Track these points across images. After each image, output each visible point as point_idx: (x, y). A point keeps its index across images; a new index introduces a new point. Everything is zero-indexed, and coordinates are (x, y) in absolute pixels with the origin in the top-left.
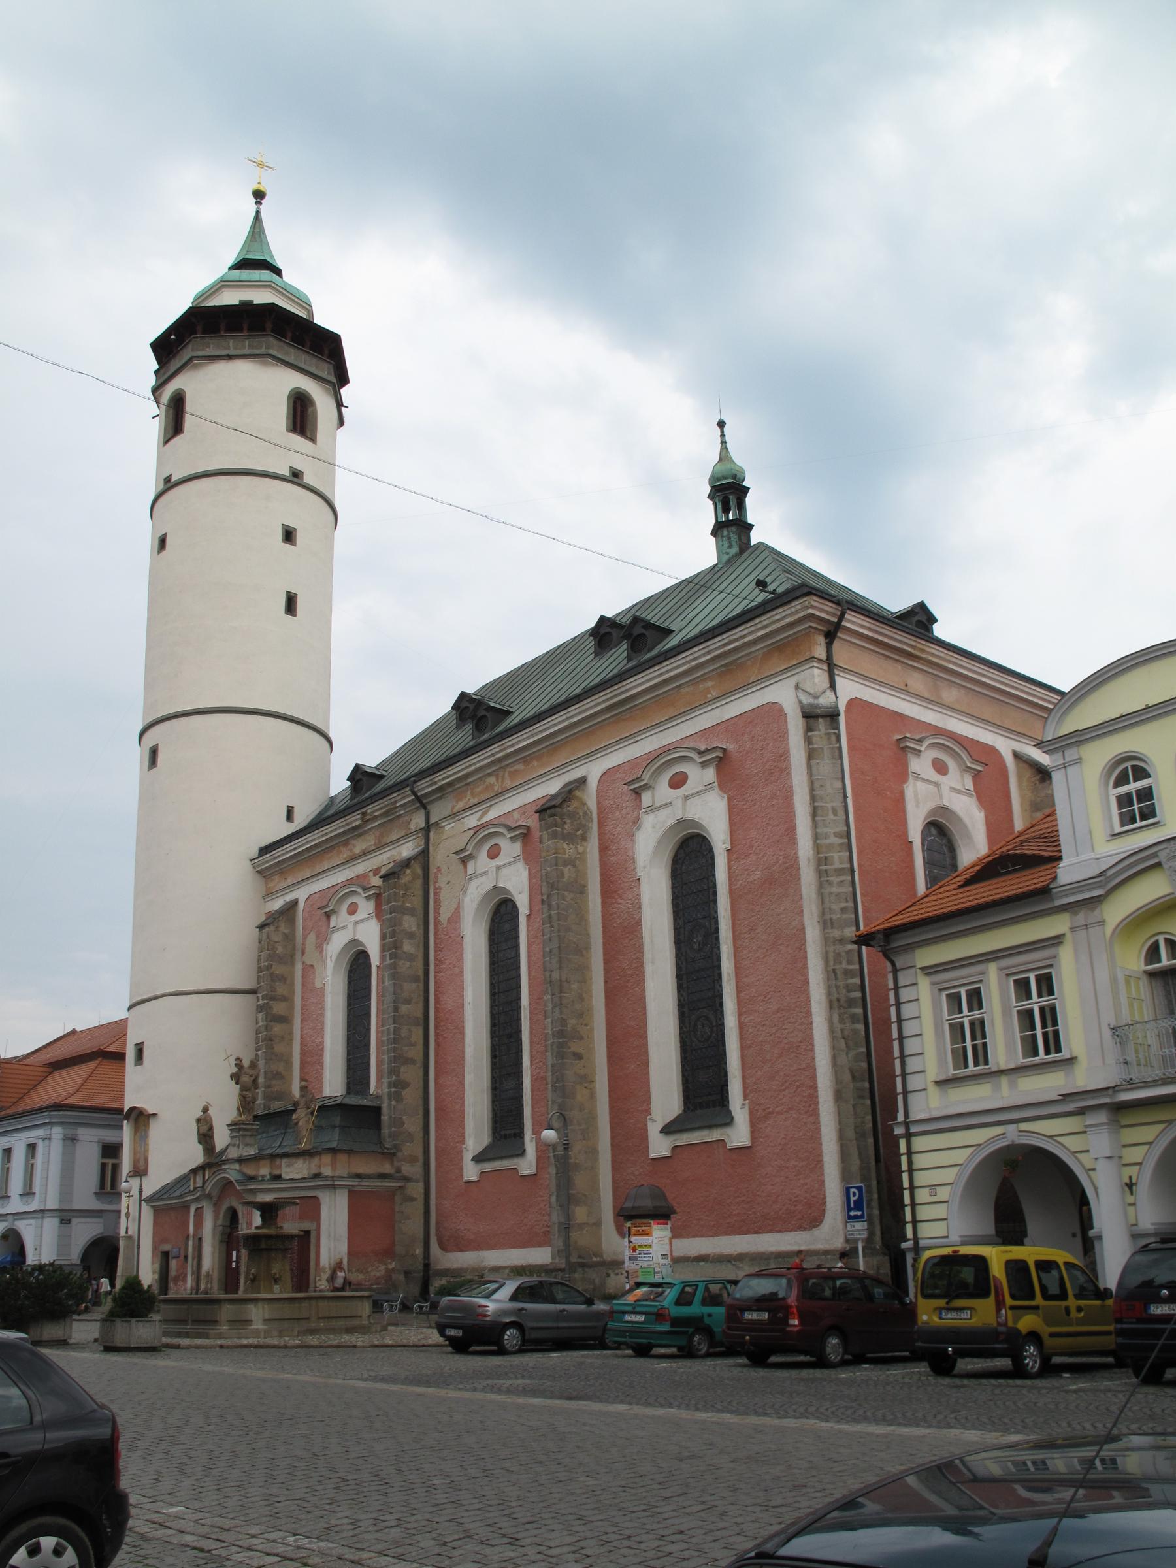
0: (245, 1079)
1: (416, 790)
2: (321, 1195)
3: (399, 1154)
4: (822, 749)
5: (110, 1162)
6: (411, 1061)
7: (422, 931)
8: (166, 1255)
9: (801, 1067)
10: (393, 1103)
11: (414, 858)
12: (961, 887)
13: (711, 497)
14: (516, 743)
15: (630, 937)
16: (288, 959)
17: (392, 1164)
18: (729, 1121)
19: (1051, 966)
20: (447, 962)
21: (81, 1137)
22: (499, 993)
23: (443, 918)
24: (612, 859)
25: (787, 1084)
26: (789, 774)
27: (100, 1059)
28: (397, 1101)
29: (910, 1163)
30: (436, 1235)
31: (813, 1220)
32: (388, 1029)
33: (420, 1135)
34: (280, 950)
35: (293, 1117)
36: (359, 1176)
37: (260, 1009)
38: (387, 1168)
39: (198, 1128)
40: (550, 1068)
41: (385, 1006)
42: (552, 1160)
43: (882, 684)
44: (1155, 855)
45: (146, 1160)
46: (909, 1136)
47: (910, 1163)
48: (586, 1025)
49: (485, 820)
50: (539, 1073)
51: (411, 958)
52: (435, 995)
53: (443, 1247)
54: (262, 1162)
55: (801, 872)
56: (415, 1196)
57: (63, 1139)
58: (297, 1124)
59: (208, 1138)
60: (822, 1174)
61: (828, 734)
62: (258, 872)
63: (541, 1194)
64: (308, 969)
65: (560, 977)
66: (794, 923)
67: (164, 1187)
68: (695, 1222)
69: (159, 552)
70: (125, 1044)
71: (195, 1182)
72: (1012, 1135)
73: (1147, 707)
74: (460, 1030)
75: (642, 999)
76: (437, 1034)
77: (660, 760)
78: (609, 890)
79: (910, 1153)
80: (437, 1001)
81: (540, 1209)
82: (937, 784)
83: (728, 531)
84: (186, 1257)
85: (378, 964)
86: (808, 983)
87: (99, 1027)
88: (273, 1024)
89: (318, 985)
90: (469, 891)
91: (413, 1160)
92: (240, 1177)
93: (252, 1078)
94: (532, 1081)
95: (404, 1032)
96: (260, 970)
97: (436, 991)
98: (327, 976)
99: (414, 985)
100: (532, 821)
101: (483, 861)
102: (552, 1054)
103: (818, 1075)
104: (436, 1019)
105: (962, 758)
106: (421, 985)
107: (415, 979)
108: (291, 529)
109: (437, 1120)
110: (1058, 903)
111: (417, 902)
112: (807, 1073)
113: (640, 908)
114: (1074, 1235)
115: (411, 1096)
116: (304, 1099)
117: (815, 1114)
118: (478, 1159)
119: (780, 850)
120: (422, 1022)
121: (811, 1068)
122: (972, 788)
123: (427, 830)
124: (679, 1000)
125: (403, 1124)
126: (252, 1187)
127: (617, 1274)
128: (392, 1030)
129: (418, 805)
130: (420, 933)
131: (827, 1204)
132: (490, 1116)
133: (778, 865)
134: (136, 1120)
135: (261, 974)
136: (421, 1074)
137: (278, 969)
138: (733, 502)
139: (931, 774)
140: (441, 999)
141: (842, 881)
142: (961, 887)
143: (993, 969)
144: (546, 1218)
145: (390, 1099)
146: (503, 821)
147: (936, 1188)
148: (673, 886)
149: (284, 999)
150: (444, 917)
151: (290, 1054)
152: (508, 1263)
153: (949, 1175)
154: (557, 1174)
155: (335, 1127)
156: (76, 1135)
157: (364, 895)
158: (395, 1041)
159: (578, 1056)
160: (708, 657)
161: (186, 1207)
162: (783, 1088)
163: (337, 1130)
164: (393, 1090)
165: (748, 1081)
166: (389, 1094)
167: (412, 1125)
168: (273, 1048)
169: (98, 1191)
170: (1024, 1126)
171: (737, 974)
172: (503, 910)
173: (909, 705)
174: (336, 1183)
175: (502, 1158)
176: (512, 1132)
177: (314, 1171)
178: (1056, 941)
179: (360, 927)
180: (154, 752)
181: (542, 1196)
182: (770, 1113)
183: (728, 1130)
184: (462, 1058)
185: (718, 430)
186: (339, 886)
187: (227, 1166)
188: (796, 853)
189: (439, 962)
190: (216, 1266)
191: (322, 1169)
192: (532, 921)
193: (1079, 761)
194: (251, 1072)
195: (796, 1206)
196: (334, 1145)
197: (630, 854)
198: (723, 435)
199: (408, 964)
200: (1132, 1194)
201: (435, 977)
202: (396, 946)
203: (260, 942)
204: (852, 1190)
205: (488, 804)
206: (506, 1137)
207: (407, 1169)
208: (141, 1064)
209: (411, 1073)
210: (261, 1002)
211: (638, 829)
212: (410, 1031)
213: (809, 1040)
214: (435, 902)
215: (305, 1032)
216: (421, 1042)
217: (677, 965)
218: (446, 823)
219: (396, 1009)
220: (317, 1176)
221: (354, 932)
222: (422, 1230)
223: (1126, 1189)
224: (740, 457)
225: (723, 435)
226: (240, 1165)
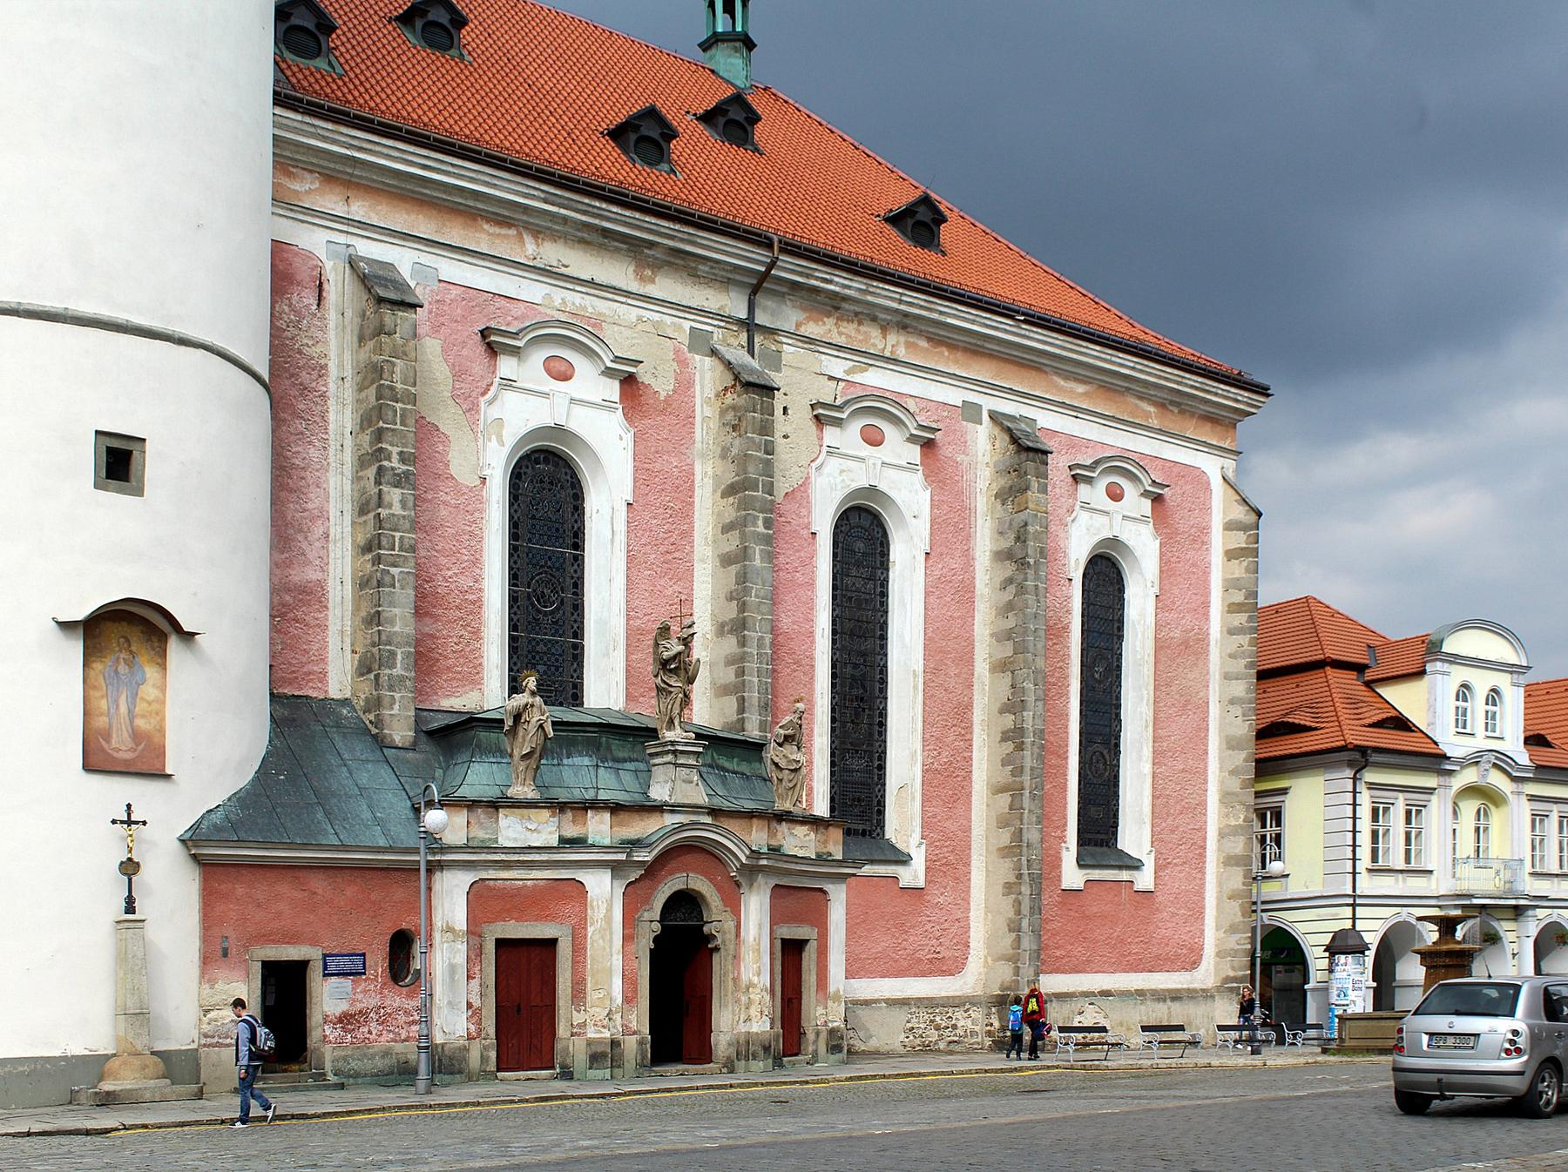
2: (828, 887)
42: (1026, 878)
102: (1032, 754)
117: (1202, 871)
121: (1202, 830)
152: (887, 995)
172: (854, 520)
182: (1169, 863)
183: (1135, 873)
213: (1203, 804)
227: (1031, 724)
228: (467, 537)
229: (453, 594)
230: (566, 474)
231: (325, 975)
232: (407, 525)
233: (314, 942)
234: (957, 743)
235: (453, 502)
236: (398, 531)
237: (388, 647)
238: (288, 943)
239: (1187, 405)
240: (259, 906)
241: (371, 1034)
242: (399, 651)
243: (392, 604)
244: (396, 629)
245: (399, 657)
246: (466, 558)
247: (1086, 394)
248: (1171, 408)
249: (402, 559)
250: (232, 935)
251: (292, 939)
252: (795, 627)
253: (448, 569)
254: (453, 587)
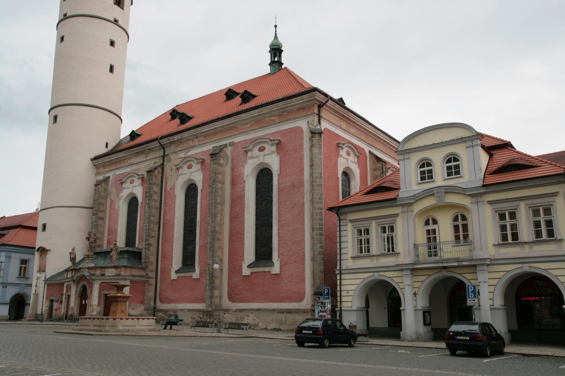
0: (92, 239)
1: (160, 142)
3: (148, 269)
4: (316, 144)
5: (23, 266)
6: (153, 237)
7: (160, 192)
8: (52, 301)
9: (300, 249)
10: (147, 251)
11: (159, 166)
12: (363, 195)
13: (270, 52)
14: (202, 130)
15: (240, 201)
16: (106, 198)
17: (145, 272)
18: (272, 265)
19: (394, 223)
21: (13, 257)
22: (188, 215)
23: (168, 188)
24: (235, 173)
25: (294, 254)
26: (303, 151)
27: (20, 228)
28: (148, 250)
29: (340, 283)
30: (159, 297)
31: (300, 298)
32: (146, 225)
33: (155, 263)
34: (102, 194)
35: (111, 254)
36: (134, 276)
37: (94, 214)
38: (143, 273)
39: (70, 256)
40: (209, 243)
41: (145, 217)
42: (208, 274)
43: (334, 124)
44: (433, 191)
45: (45, 266)
46: (341, 274)
47: (340, 283)
48: (222, 229)
49: (187, 155)
50: (202, 244)
51: (155, 201)
52: (164, 214)
53: (161, 301)
54: (98, 269)
55: (305, 184)
56: (152, 284)
57: (6, 257)
58: (112, 256)
59: (74, 260)
60: (305, 284)
61: (319, 139)
62: (94, 165)
63: (201, 285)
64: (112, 202)
65: (215, 212)
66: (301, 201)
67: (52, 276)
68: (257, 297)
69: (60, 42)
70: (37, 224)
71: (67, 275)
72: (377, 276)
73: (434, 144)
74: (172, 227)
75: (243, 222)
76: (163, 228)
77: (255, 141)
78: (234, 183)
79: (340, 280)
80: (164, 217)
82: (347, 159)
83: (275, 64)
84: (61, 302)
85: (141, 202)
86: (304, 221)
87: (16, 216)
88: (99, 220)
89: (116, 208)
90: (179, 179)
91: (152, 271)
92: (88, 274)
93: (94, 239)
94: (199, 247)
95: (152, 226)
96: (94, 200)
97: (164, 213)
98: (120, 205)
99: (156, 211)
100: (208, 159)
101: (185, 170)
102: (210, 238)
103: (305, 252)
104: (163, 223)
105: (355, 152)
106: (159, 211)
107: (157, 209)
108: (113, 41)
109: (162, 258)
110: (398, 203)
111: (159, 182)
112: (301, 251)
113: (244, 191)
114: (385, 308)
115: (153, 249)
116: (115, 248)
118: (177, 272)
119: (298, 176)
120: (158, 223)
122: (357, 162)
123: (164, 156)
124: (256, 223)
125: (150, 258)
126: (94, 278)
127: (228, 314)
128: (147, 225)
129: (161, 147)
130: (159, 192)
131: (306, 294)
132: (182, 257)
133: (296, 181)
134: (41, 252)
135: (95, 202)
136: (156, 241)
137: (102, 201)
138: (278, 55)
139: (346, 156)
140: (166, 216)
141: (320, 189)
142: (363, 195)
143: (374, 223)
144: (202, 293)
145: (145, 250)
146: (194, 156)
147: (349, 291)
148: (257, 185)
149: (103, 211)
150: (168, 188)
151: (104, 231)
152: (187, 308)
153: (354, 287)
154: (209, 279)
155: (125, 258)
156: (11, 256)
157: (137, 177)
158: (149, 229)
159: (219, 240)
160: (277, 108)
161: (63, 284)
162: (293, 255)
163: (126, 259)
164: (147, 246)
165: (280, 252)
166: (145, 248)
167: (153, 259)
168: (98, 229)
169: (18, 276)
170: (380, 273)
171: (279, 216)
172: (191, 187)
173: (341, 132)
174: (126, 278)
175: (186, 272)
176: (190, 263)
177: (118, 273)
178: (397, 215)
179: (134, 188)
180: (56, 118)
182: (288, 263)
183: (272, 268)
184: (173, 237)
185: (275, 28)
186: (127, 173)
187: (83, 270)
188: (303, 178)
189: (165, 203)
190: (76, 305)
191: (121, 273)
192: (203, 192)
193: (409, 158)
194: (94, 237)
195: (294, 294)
196: (125, 264)
197: (242, 172)
198: (276, 31)
199: (154, 203)
200: (415, 297)
201: (164, 208)
202: (151, 196)
203: (95, 191)
204: (325, 290)
205: (189, 150)
206: (187, 265)
207: (150, 274)
208: (45, 231)
209: (153, 241)
210: (94, 212)
211: (246, 164)
212: (154, 226)
213: (303, 240)
214: (165, 182)
216: (157, 230)
217: (256, 211)
218: (172, 155)
219: (149, 218)
220: (119, 275)
221: (132, 190)
222: (154, 295)
223: (414, 295)
224: (281, 40)
225: (276, 31)
226: (89, 270)
227: (210, 229)
239: (288, 110)
247: (251, 126)
248: (283, 114)
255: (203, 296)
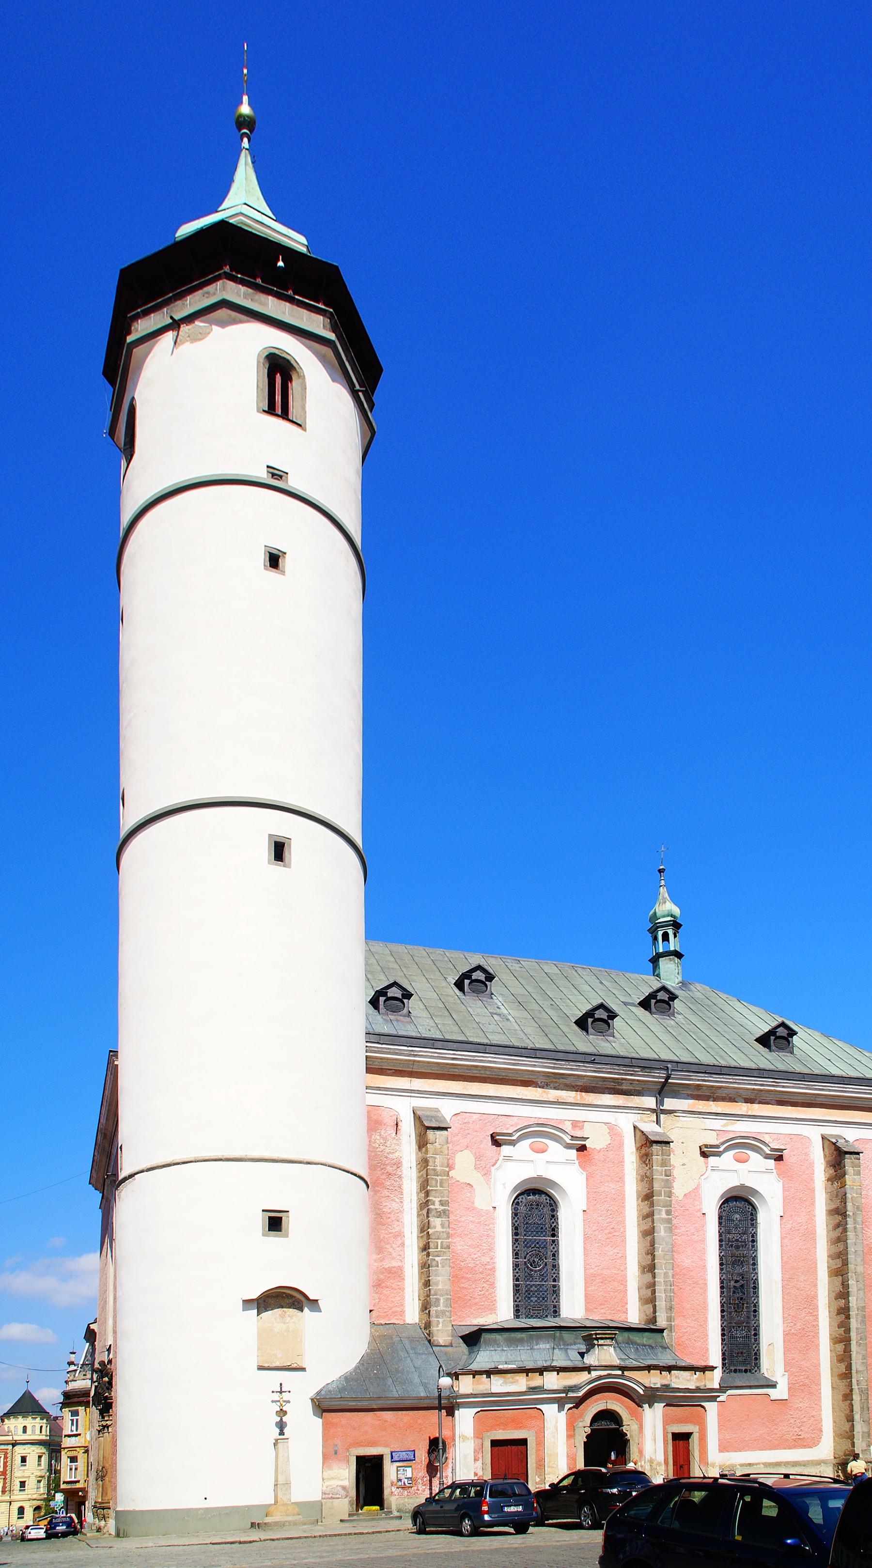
20: (683, 1229)
50: (791, 1330)
63: (792, 1413)
81: (791, 1423)
140: (676, 1257)
144: (797, 1429)
181: (791, 1415)
215: (459, 1248)
228: (486, 1237)
229: (478, 1267)
230: (546, 1199)
231: (392, 1462)
232: (445, 1236)
233: (386, 1446)
234: (807, 1318)
235: (476, 1221)
236: (438, 1239)
237: (435, 1297)
238: (371, 1446)
240: (354, 1429)
241: (419, 1490)
242: (441, 1298)
243: (436, 1275)
244: (440, 1287)
245: (442, 1301)
246: (485, 1248)
249: (442, 1253)
250: (339, 1443)
251: (373, 1444)
252: (694, 1264)
253: (475, 1254)
254: (478, 1263)
255: (800, 1435)
